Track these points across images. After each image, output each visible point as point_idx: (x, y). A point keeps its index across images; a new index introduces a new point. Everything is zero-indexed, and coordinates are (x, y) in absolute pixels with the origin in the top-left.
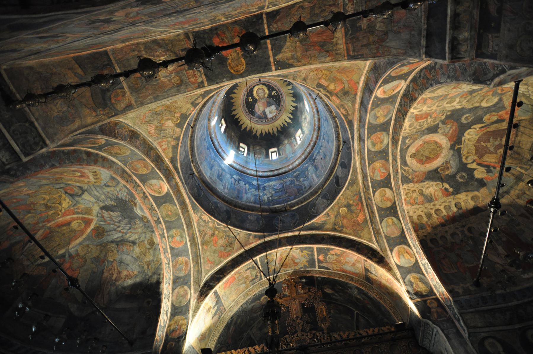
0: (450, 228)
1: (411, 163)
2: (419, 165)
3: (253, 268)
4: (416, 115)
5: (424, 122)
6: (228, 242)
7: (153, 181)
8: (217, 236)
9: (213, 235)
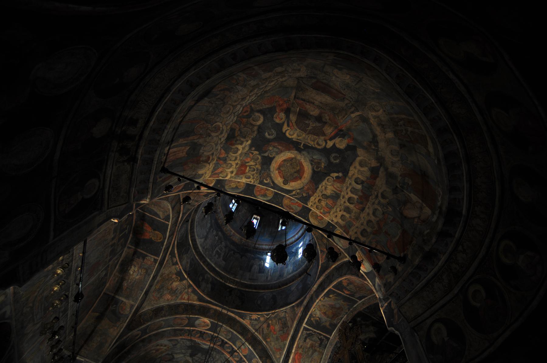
0: (368, 208)
1: (292, 187)
2: (299, 182)
3: (309, 335)
4: (236, 174)
5: (250, 168)
6: (282, 324)
7: (197, 322)
8: (272, 325)
9: (268, 326)
